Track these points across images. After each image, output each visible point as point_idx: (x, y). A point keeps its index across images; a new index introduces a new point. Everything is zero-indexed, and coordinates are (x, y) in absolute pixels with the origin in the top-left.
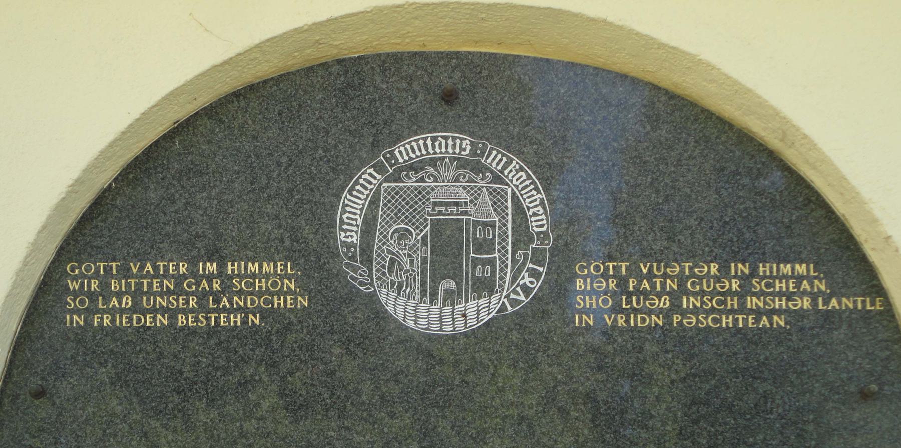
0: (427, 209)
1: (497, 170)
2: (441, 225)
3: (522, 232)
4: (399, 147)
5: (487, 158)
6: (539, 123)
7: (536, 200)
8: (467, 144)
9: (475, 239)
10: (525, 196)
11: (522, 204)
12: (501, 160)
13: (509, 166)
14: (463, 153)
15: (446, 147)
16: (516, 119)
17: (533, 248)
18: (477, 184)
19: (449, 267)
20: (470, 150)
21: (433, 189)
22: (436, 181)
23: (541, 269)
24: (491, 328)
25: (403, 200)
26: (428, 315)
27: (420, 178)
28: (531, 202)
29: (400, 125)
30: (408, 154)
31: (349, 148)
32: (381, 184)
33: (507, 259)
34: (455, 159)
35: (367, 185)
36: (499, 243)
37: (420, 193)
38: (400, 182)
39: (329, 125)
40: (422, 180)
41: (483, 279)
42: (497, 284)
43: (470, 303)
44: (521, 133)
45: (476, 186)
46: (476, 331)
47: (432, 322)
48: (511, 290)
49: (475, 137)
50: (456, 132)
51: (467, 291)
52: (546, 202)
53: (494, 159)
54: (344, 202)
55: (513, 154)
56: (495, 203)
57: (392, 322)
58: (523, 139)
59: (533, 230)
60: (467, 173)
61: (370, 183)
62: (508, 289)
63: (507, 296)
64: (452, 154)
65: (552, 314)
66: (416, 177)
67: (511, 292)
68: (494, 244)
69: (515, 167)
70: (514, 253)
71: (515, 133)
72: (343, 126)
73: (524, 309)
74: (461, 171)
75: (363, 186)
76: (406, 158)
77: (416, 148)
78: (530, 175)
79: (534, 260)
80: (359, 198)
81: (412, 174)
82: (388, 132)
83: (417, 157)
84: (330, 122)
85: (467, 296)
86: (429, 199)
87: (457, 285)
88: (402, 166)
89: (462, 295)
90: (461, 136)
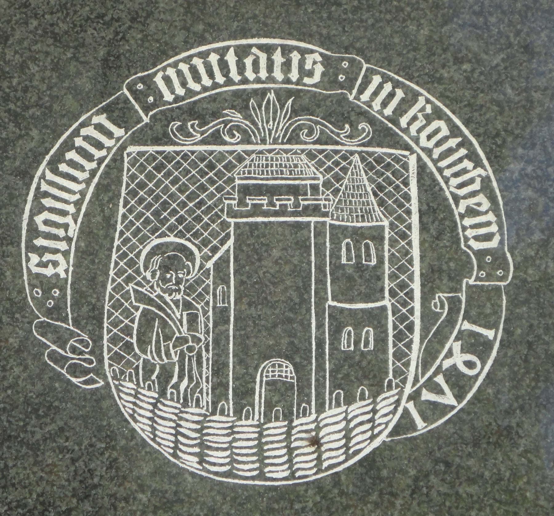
0: (227, 202)
1: (383, 116)
2: (258, 236)
3: (444, 251)
4: (164, 69)
5: (361, 91)
6: (474, 18)
7: (472, 181)
8: (315, 63)
9: (337, 267)
10: (447, 173)
11: (441, 189)
12: (391, 95)
13: (410, 107)
14: (306, 80)
15: (270, 68)
16: (423, 10)
17: (469, 287)
18: (339, 147)
19: (279, 330)
20: (323, 74)
21: (240, 159)
22: (247, 140)
23: (490, 334)
24: (379, 470)
25: (173, 183)
26: (230, 442)
27: (213, 134)
28: (461, 186)
29: (167, 21)
30: (184, 84)
31: (53, 70)
32: (123, 148)
33: (411, 311)
34: (290, 93)
35: (92, 150)
36: (393, 277)
37: (211, 167)
38: (166, 144)
39: (9, 22)
40: (216, 139)
41: (357, 358)
42: (391, 368)
43: (329, 413)
44: (436, 37)
45: (336, 152)
46: (343, 478)
47: (239, 458)
48: (422, 381)
49: (333, 47)
50: (291, 36)
51: (320, 385)
52: (495, 184)
53: (376, 94)
54: (38, 188)
55: (417, 84)
56: (381, 188)
57: (147, 458)
58: (439, 51)
59: (469, 247)
60: (317, 123)
61: (99, 146)
62: (416, 380)
63: (415, 397)
64: (283, 82)
65: (520, 437)
66: (202, 133)
67: (425, 385)
68: (380, 278)
69: (422, 109)
70: (426, 299)
71: (421, 38)
72: (39, 25)
73: (455, 424)
74: (303, 120)
75: (81, 152)
76: (180, 91)
77: (202, 70)
78: (458, 128)
79: (473, 313)
80: (74, 179)
81: (192, 126)
82: (140, 36)
83: (205, 89)
84: (11, 16)
85: (320, 396)
86: (231, 180)
87: (296, 372)
88: (172, 110)
89: (309, 395)
90: (302, 45)
